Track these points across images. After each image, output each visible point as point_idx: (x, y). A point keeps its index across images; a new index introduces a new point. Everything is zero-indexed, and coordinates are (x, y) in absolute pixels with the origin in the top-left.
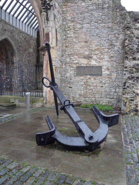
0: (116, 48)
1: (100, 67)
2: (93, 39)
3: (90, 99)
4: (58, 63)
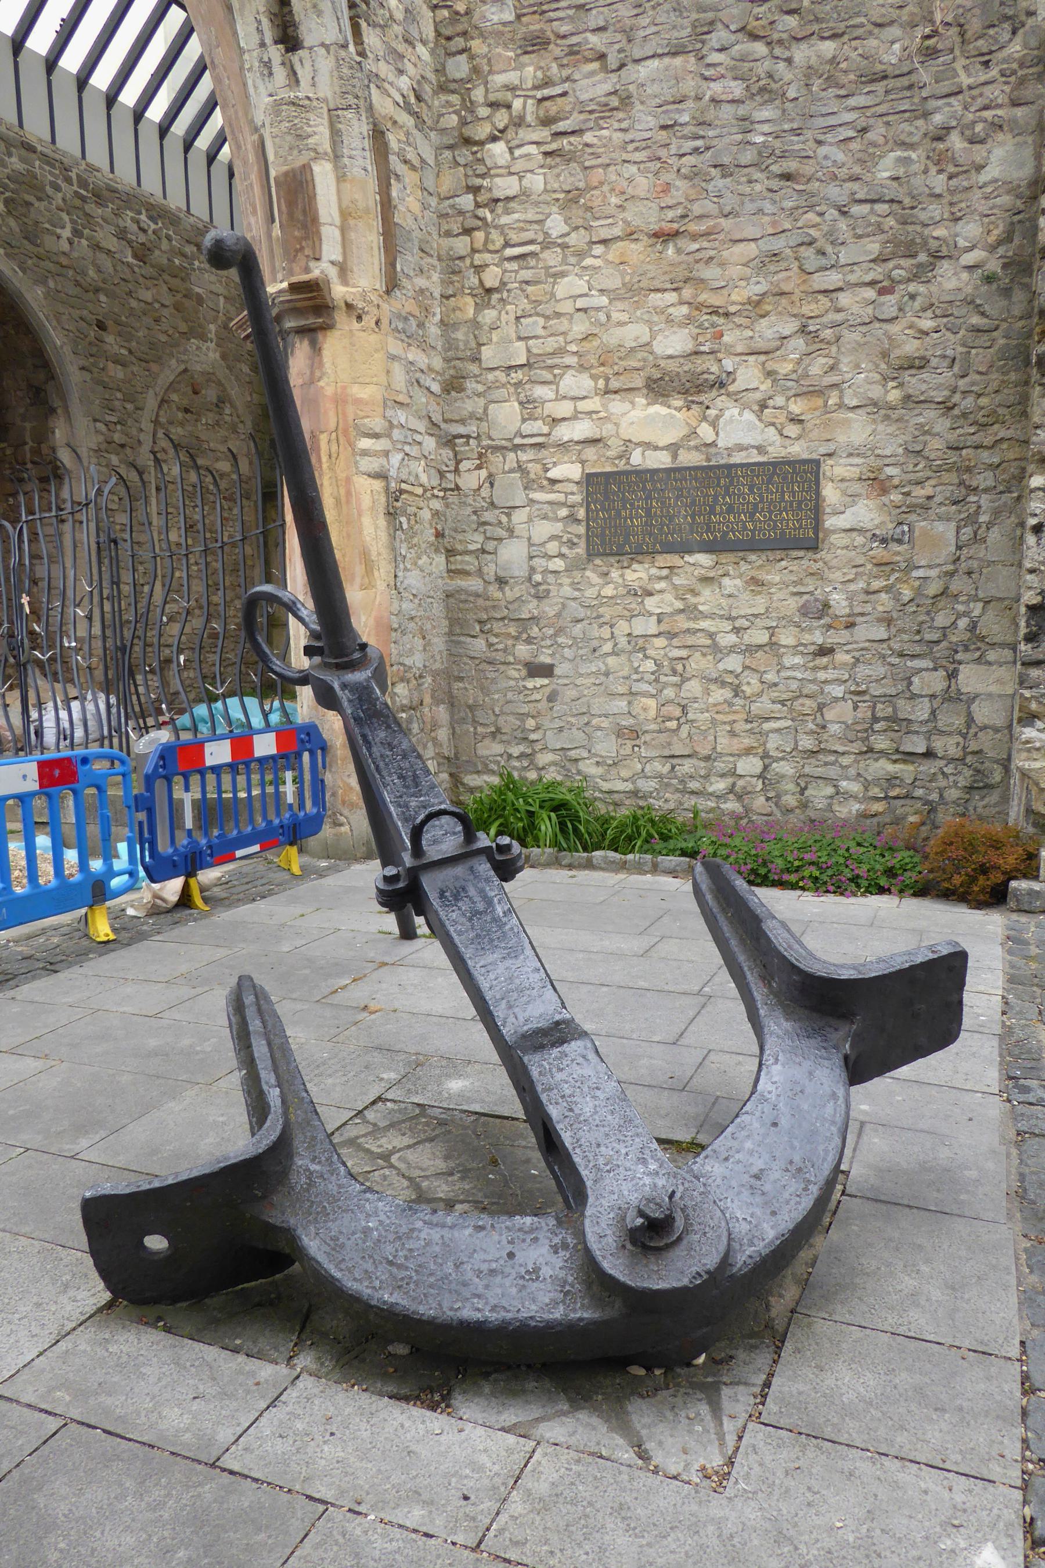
0: (951, 280)
1: (806, 473)
2: (729, 202)
3: (720, 766)
4: (414, 451)
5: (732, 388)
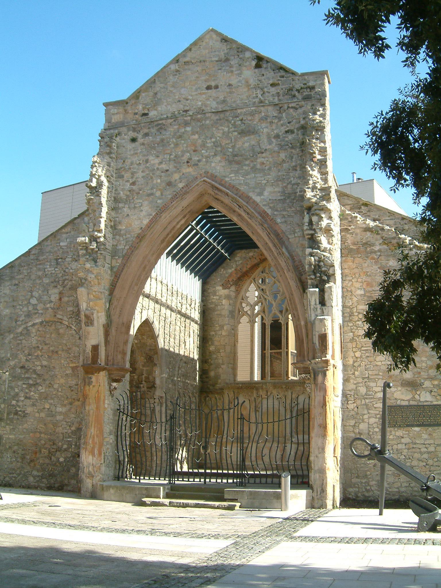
5: (423, 386)
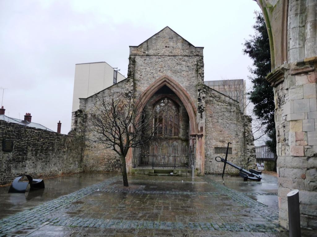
0: (240, 137)
